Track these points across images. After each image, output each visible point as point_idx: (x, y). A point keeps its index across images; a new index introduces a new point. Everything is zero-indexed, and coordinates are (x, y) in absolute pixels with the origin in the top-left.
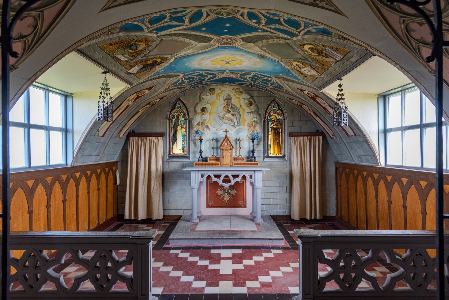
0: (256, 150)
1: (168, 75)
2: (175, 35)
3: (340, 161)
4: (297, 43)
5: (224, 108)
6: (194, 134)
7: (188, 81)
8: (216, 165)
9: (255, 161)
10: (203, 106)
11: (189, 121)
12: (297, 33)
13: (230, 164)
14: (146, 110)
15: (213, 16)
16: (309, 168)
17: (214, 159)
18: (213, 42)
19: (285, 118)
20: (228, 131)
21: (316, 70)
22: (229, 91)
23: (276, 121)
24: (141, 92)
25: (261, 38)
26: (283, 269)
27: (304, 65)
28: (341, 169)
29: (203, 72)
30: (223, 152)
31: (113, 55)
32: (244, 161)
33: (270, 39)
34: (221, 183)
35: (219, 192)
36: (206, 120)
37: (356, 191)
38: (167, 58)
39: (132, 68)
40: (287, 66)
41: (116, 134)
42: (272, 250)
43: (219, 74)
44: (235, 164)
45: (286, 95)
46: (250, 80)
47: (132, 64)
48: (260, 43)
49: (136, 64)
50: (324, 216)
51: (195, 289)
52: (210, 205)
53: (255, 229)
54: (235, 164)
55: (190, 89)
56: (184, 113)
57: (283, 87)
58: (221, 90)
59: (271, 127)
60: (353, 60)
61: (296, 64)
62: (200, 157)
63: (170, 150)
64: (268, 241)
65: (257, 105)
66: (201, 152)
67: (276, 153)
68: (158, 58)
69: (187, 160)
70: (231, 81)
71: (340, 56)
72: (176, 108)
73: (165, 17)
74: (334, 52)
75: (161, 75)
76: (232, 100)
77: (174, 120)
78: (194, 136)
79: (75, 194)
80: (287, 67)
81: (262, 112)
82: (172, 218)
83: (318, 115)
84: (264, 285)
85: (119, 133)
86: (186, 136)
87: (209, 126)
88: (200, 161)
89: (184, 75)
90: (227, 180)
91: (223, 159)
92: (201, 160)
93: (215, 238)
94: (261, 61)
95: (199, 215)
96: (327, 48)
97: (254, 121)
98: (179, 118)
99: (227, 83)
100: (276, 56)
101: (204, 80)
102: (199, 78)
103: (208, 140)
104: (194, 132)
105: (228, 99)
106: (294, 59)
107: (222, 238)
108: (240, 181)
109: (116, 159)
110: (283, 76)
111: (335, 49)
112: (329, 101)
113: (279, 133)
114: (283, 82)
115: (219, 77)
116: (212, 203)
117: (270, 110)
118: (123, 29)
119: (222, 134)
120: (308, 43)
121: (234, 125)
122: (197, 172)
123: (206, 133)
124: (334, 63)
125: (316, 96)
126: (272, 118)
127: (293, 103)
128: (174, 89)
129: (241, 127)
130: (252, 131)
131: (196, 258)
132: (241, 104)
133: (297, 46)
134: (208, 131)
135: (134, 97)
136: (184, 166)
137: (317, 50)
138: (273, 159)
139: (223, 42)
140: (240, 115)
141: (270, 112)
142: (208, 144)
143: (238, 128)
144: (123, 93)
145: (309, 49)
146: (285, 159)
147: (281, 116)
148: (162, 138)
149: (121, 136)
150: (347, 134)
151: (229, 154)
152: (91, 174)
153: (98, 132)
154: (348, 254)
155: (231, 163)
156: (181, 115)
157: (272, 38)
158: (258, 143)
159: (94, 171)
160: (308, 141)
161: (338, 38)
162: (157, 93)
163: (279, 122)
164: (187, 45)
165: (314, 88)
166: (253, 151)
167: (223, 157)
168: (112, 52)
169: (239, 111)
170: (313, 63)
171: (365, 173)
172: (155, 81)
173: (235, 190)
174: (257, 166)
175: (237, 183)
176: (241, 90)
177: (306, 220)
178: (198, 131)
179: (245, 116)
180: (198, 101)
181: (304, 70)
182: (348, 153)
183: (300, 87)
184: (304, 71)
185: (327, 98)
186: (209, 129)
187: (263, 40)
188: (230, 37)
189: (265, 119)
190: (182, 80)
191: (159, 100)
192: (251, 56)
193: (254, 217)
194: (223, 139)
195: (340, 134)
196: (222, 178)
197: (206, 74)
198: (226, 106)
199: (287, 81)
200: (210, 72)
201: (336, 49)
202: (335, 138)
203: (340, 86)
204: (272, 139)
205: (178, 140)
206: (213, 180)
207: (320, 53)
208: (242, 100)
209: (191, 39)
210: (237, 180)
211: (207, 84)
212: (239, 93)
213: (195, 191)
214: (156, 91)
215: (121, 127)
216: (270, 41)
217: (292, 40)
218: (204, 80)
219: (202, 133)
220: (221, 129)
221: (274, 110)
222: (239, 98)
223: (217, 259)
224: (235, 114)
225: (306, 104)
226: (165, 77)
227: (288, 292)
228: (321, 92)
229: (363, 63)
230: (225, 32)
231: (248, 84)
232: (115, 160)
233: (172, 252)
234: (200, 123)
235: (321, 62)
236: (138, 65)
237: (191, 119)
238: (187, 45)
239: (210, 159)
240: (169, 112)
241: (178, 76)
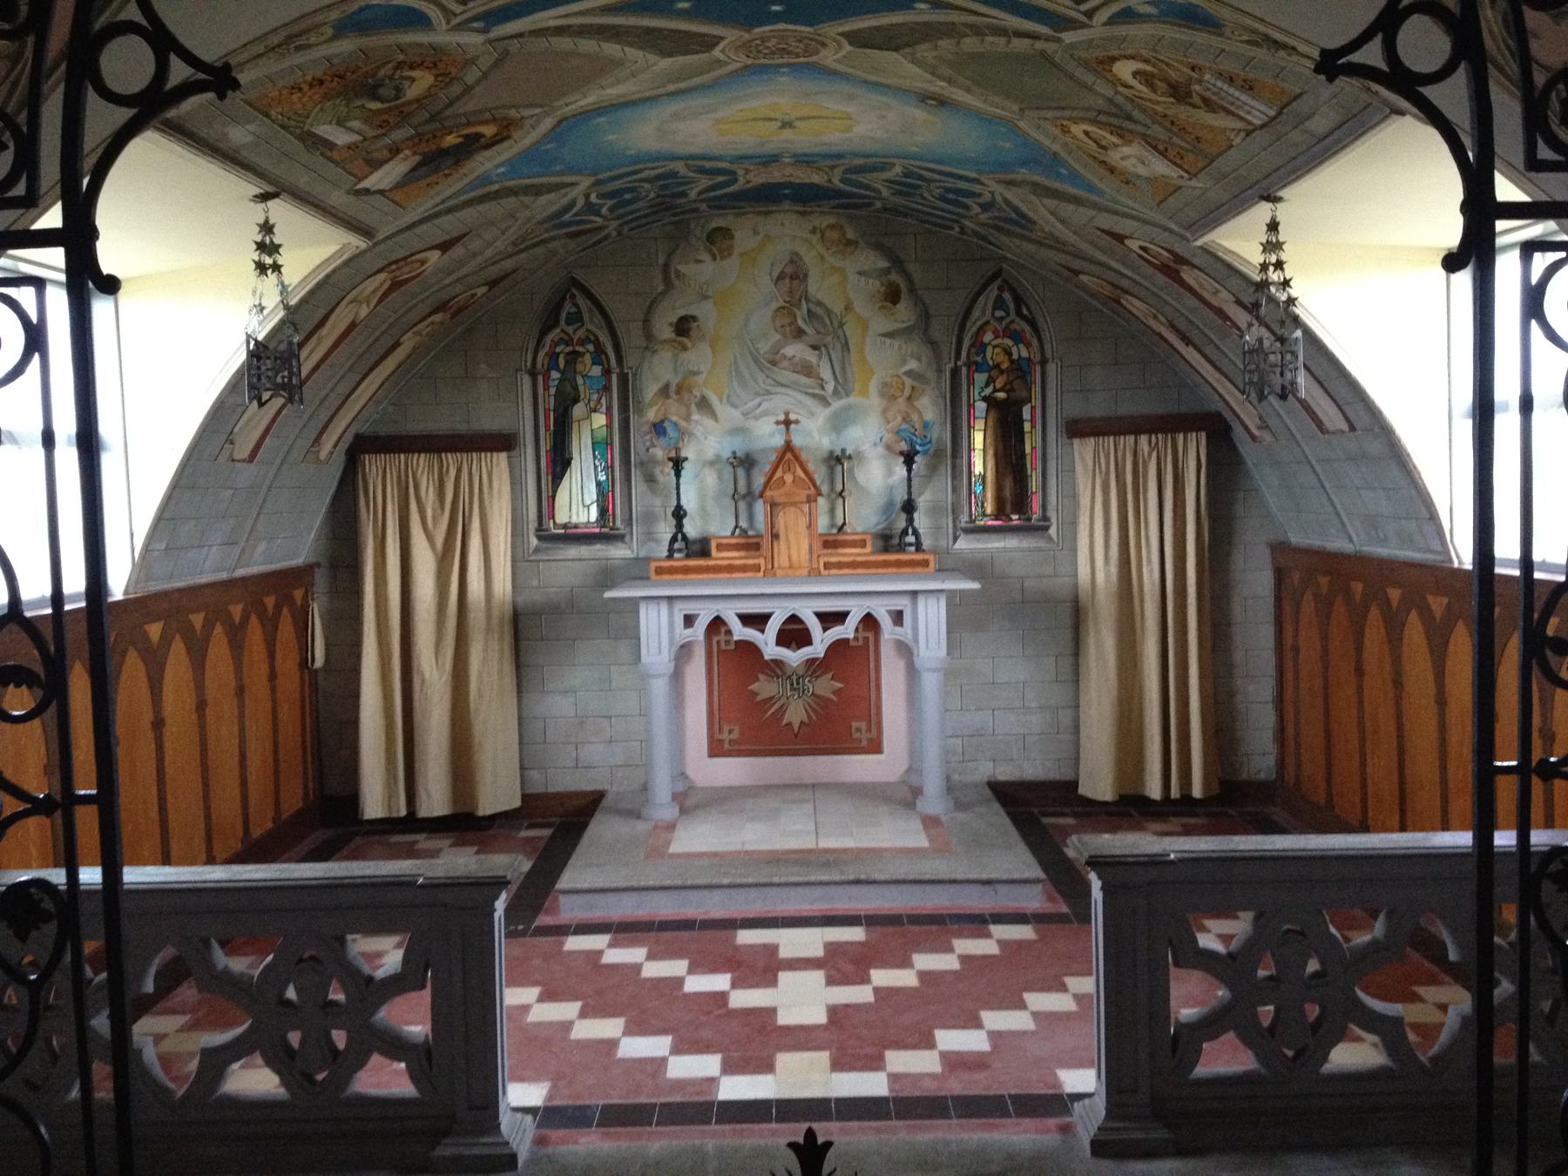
0: (923, 501)
1: (528, 186)
2: (560, 31)
3: (1296, 539)
4: (1083, 54)
5: (774, 318)
6: (648, 437)
7: (610, 203)
8: (744, 569)
9: (918, 546)
10: (682, 312)
11: (623, 379)
12: (1082, 18)
13: (805, 564)
16: (1157, 575)
17: (738, 544)
18: (723, 51)
19: (1048, 354)
20: (797, 422)
21: (1172, 157)
22: (795, 237)
23: (1008, 371)
24: (412, 262)
25: (928, 33)
26: (1040, 1001)
27: (1121, 136)
28: (1296, 576)
29: (679, 167)
30: (775, 513)
31: (302, 128)
32: (868, 549)
33: (968, 35)
34: (769, 647)
35: (764, 687)
36: (697, 373)
37: (1359, 671)
38: (522, 118)
39: (376, 169)
40: (1045, 136)
42: (993, 928)
43: (747, 171)
44: (827, 566)
45: (1045, 254)
46: (885, 193)
47: (376, 155)
48: (924, 51)
49: (395, 151)
50: (1223, 783)
51: (681, 1084)
52: (726, 746)
53: (920, 840)
54: (827, 566)
55: (619, 234)
56: (597, 343)
57: (1034, 223)
58: (759, 238)
59: (984, 399)
60: (1320, 124)
61: (1086, 133)
62: (674, 540)
63: (546, 505)
64: (979, 888)
65: (921, 300)
66: (679, 514)
67: (1008, 508)
68: (487, 122)
69: (618, 552)
70: (805, 197)
71: (1263, 108)
72: (562, 323)
74: (1237, 94)
75: (496, 187)
76: (810, 281)
77: (555, 375)
78: (648, 443)
79: (148, 717)
80: (1047, 143)
82: (562, 804)
83: (1196, 340)
84: (954, 1062)
86: (609, 443)
87: (713, 399)
88: (676, 555)
89: (597, 183)
90: (794, 634)
91: (775, 544)
92: (680, 550)
93: (750, 880)
94: (931, 118)
95: (680, 787)
96: (1207, 77)
97: (909, 373)
98: (580, 367)
99: (786, 205)
100: (996, 99)
101: (683, 194)
102: (662, 188)
103: (712, 464)
104: (645, 428)
105: (793, 275)
106: (1075, 113)
107: (783, 880)
108: (851, 636)
109: (304, 554)
110: (1036, 178)
111: (1240, 82)
112: (1235, 282)
113: (1021, 421)
114: (1033, 198)
115: (748, 182)
116: (732, 737)
117: (978, 319)
118: (342, 29)
119: (767, 435)
120: (1128, 52)
121: (823, 393)
122: (664, 608)
123: (698, 431)
124: (1242, 134)
125: (1181, 260)
126: (989, 357)
127: (1083, 287)
128: (553, 238)
129: (852, 400)
130: (899, 419)
131: (675, 967)
133: (1085, 64)
134: (708, 422)
135: (382, 285)
136: (608, 576)
137: (1164, 80)
138: (994, 537)
139: (766, 51)
140: (846, 346)
141: (981, 330)
142: (711, 478)
143: (837, 405)
144: (334, 271)
145: (1134, 77)
146: (1050, 538)
147: (1028, 345)
148: (502, 457)
149: (323, 455)
150: (1319, 424)
151: (803, 521)
152: (208, 626)
153: (232, 443)
154: (1289, 931)
155: (811, 560)
156: (588, 356)
157: (977, 31)
159: (217, 614)
160: (1155, 454)
161: (1248, 42)
162: (479, 260)
163: (1020, 373)
164: (612, 64)
165: (1166, 229)
166: (909, 507)
167: (775, 536)
168: (299, 115)
169: (840, 332)
170: (1157, 131)
171: (1395, 594)
172: (468, 214)
173: (830, 676)
174: (927, 570)
175: (839, 646)
176: (850, 235)
177: (1147, 801)
178: (662, 422)
179: (867, 349)
180: (661, 288)
181: (1121, 155)
182: (1327, 503)
183: (1106, 221)
184: (1122, 159)
185: (1226, 270)
186: (714, 415)
187: (941, 39)
188: (796, 31)
189: (959, 363)
191: (484, 289)
192: (884, 99)
193: (917, 792)
194: (773, 458)
195: (1288, 421)
196: (773, 626)
197: (692, 171)
198: (783, 308)
199: (1048, 196)
200: (708, 165)
201: (1245, 81)
202: (1267, 437)
203: (1273, 226)
204: (991, 452)
205: (575, 464)
206: (736, 638)
207: (1180, 93)
208: (853, 277)
209: (631, 45)
210: (837, 632)
211: (696, 210)
212: (841, 248)
213: (660, 688)
214: (475, 255)
215: (324, 417)
216: (970, 44)
217: (1059, 40)
218: (683, 194)
219: (683, 434)
220: (766, 413)
221: (1001, 319)
222: (841, 270)
223: (765, 967)
224: (825, 346)
225: (1136, 290)
226: (513, 192)
227: (1054, 1087)
228: (1201, 247)
229: (1356, 139)
230: (776, 12)
231: (879, 205)
232: (298, 561)
233: (575, 943)
234: (673, 388)
235: (1189, 129)
236: (401, 156)
237: (631, 368)
238: (606, 67)
239: (720, 547)
240: (532, 346)
241: (573, 184)
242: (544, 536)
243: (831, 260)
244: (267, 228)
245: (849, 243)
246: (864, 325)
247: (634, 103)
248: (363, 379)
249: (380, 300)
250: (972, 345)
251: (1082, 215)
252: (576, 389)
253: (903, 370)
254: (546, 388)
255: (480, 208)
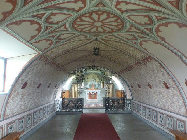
90: (93, 93)
105: (93, 76)
119: (92, 83)
158: (99, 85)
175: (95, 93)
213: (86, 95)
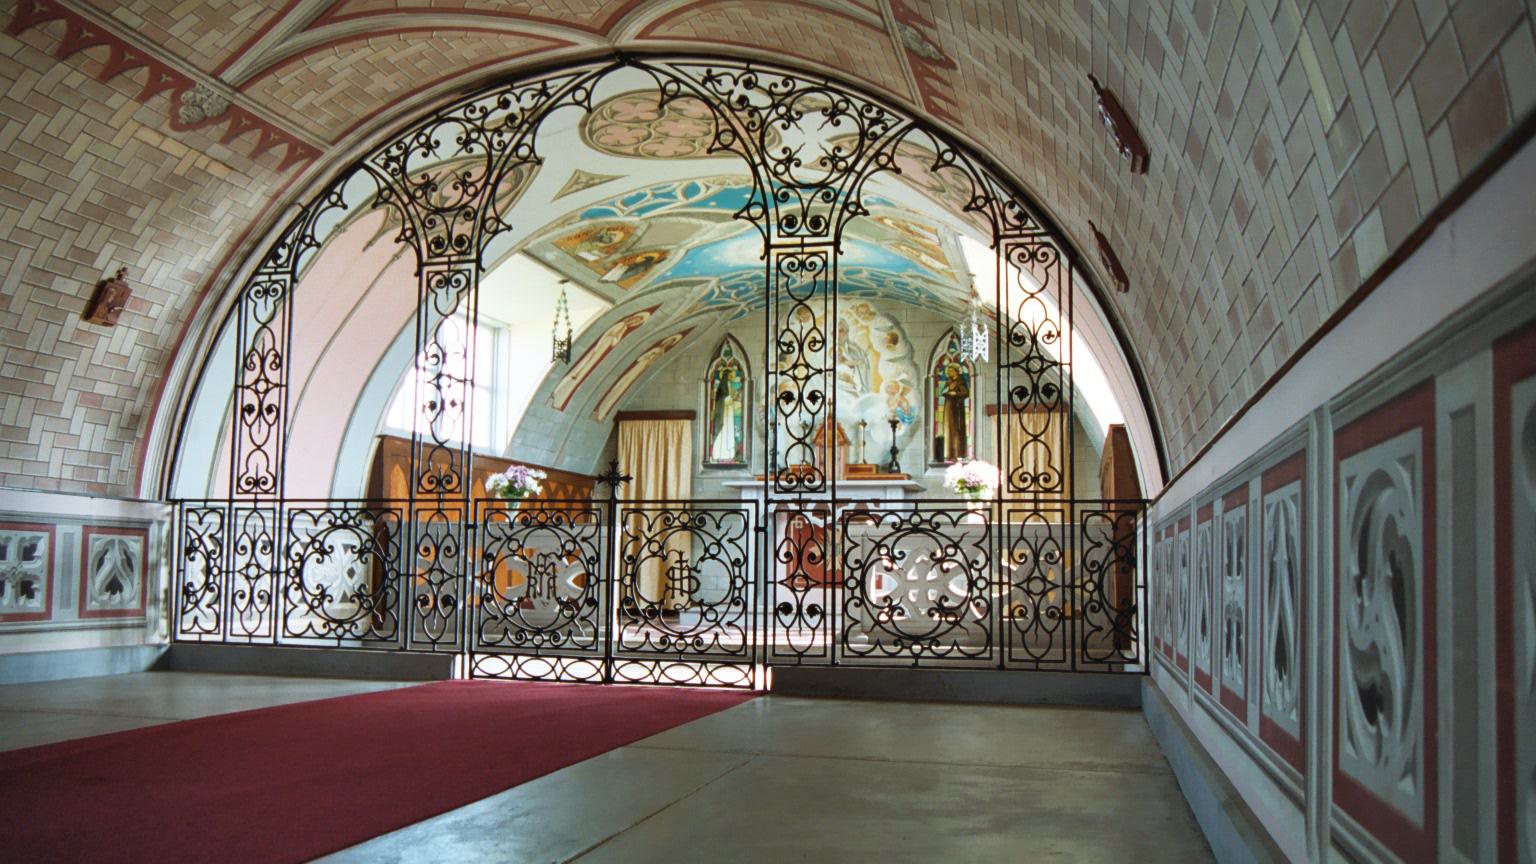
2: (669, 215)
11: (751, 384)
14: (655, 360)
15: (714, 189)
19: (978, 372)
41: (589, 410)
49: (615, 264)
55: (750, 310)
56: (739, 365)
59: (945, 395)
63: (708, 449)
67: (956, 453)
73: (645, 195)
75: (669, 282)
81: (921, 358)
85: (597, 408)
86: (742, 417)
89: (721, 281)
113: (962, 404)
118: (583, 218)
128: (711, 310)
129: (872, 394)
132: (872, 340)
140: (868, 367)
143: (863, 397)
148: (687, 424)
149: (600, 418)
158: (912, 434)
172: (660, 295)
176: (872, 309)
190: (721, 291)
205: (724, 428)
208: (873, 331)
215: (600, 396)
222: (867, 327)
226: (680, 284)
242: (708, 466)
243: (863, 323)
244: (564, 294)
245: (873, 314)
246: (877, 355)
247: (716, 243)
248: (619, 379)
249: (624, 336)
250: (937, 367)
251: (944, 290)
252: (727, 389)
253: (898, 379)
254: (712, 388)
255: (665, 291)
